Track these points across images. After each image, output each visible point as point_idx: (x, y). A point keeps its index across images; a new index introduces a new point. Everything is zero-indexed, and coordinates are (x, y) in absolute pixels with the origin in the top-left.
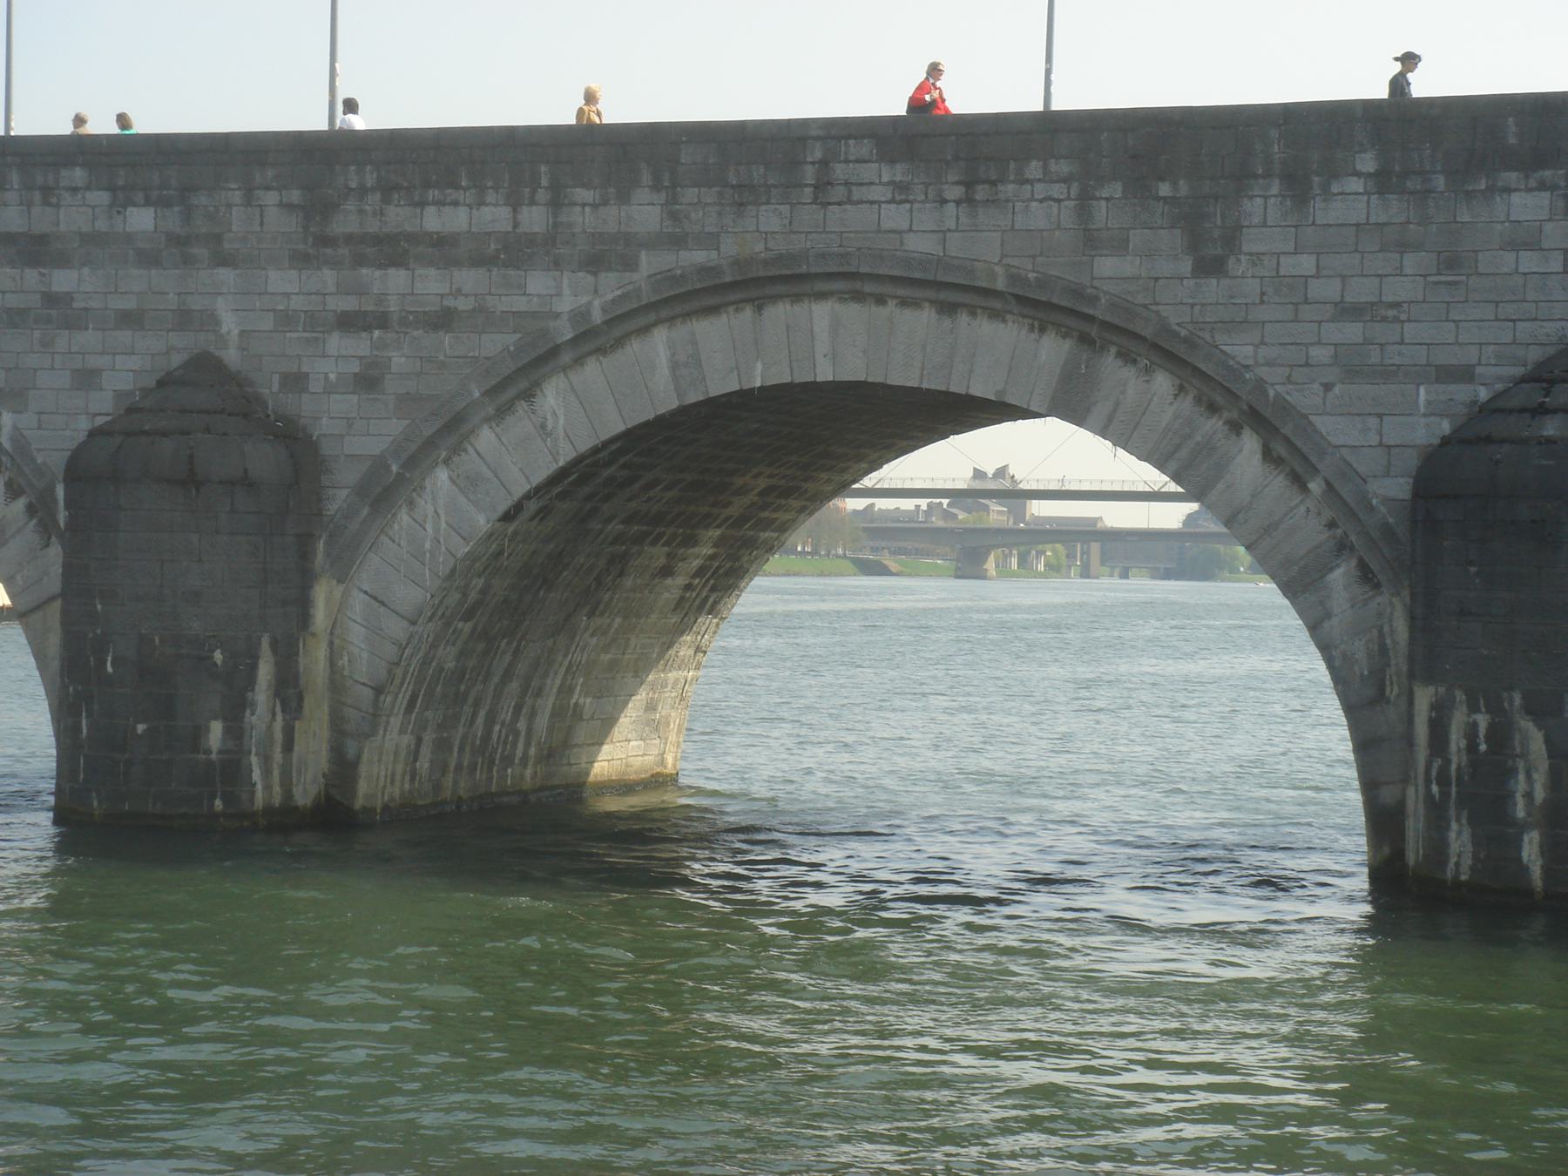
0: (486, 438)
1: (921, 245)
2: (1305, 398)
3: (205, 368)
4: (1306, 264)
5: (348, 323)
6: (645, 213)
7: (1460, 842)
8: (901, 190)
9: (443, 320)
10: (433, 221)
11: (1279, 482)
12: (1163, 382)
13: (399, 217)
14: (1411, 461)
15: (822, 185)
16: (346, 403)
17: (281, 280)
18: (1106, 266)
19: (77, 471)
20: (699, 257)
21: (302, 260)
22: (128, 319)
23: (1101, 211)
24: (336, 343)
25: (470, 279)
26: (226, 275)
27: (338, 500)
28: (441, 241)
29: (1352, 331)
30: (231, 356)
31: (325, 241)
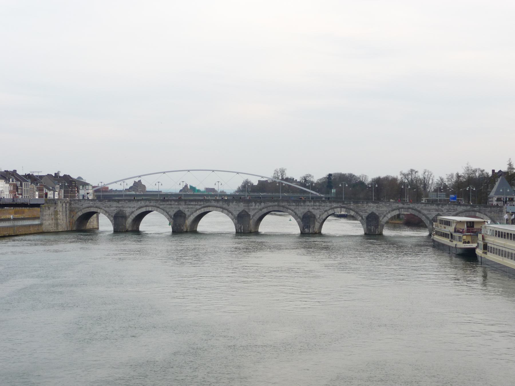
0: (194, 214)
1: (215, 205)
2: (233, 212)
3: (180, 211)
4: (232, 206)
5: (187, 208)
6: (202, 203)
7: (239, 230)
8: (214, 202)
9: (192, 208)
10: (191, 203)
11: (232, 215)
12: (226, 211)
13: (190, 203)
14: (237, 215)
15: (211, 202)
16: (187, 212)
17: (184, 206)
18: (224, 206)
19: (175, 215)
20: (205, 205)
21: (184, 205)
22: (176, 208)
23: (224, 203)
24: (186, 209)
25: (193, 206)
26: (181, 206)
27: (187, 217)
28: (192, 204)
29: (235, 209)
30: (181, 210)
31: (186, 204)
